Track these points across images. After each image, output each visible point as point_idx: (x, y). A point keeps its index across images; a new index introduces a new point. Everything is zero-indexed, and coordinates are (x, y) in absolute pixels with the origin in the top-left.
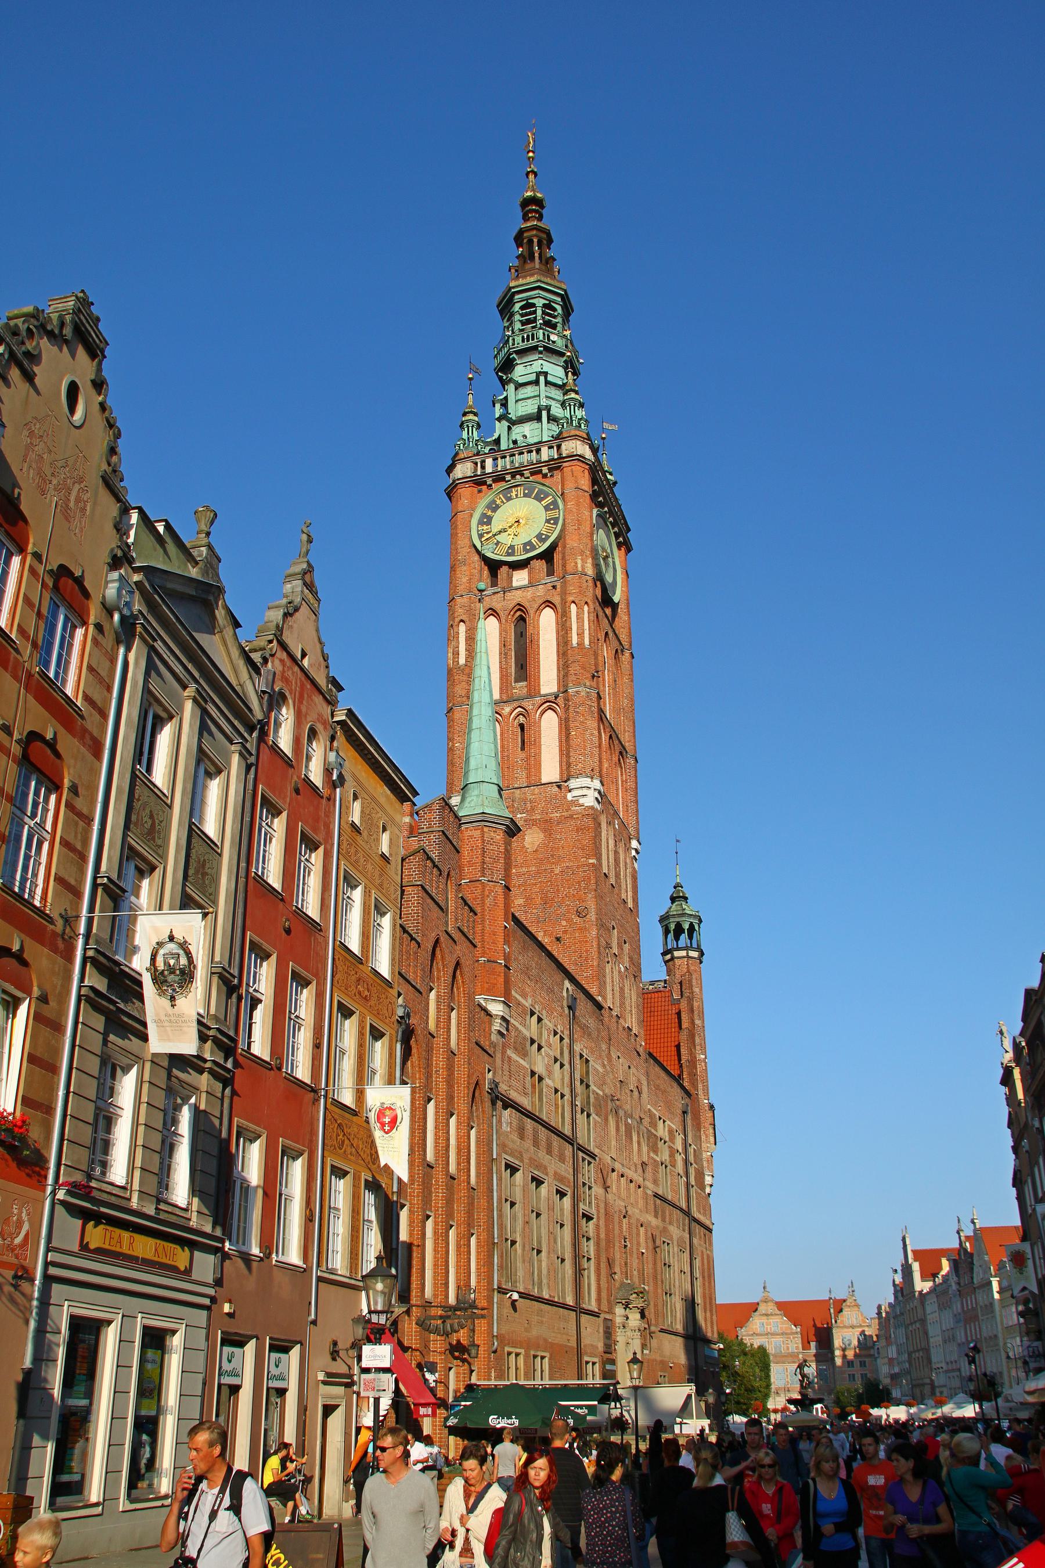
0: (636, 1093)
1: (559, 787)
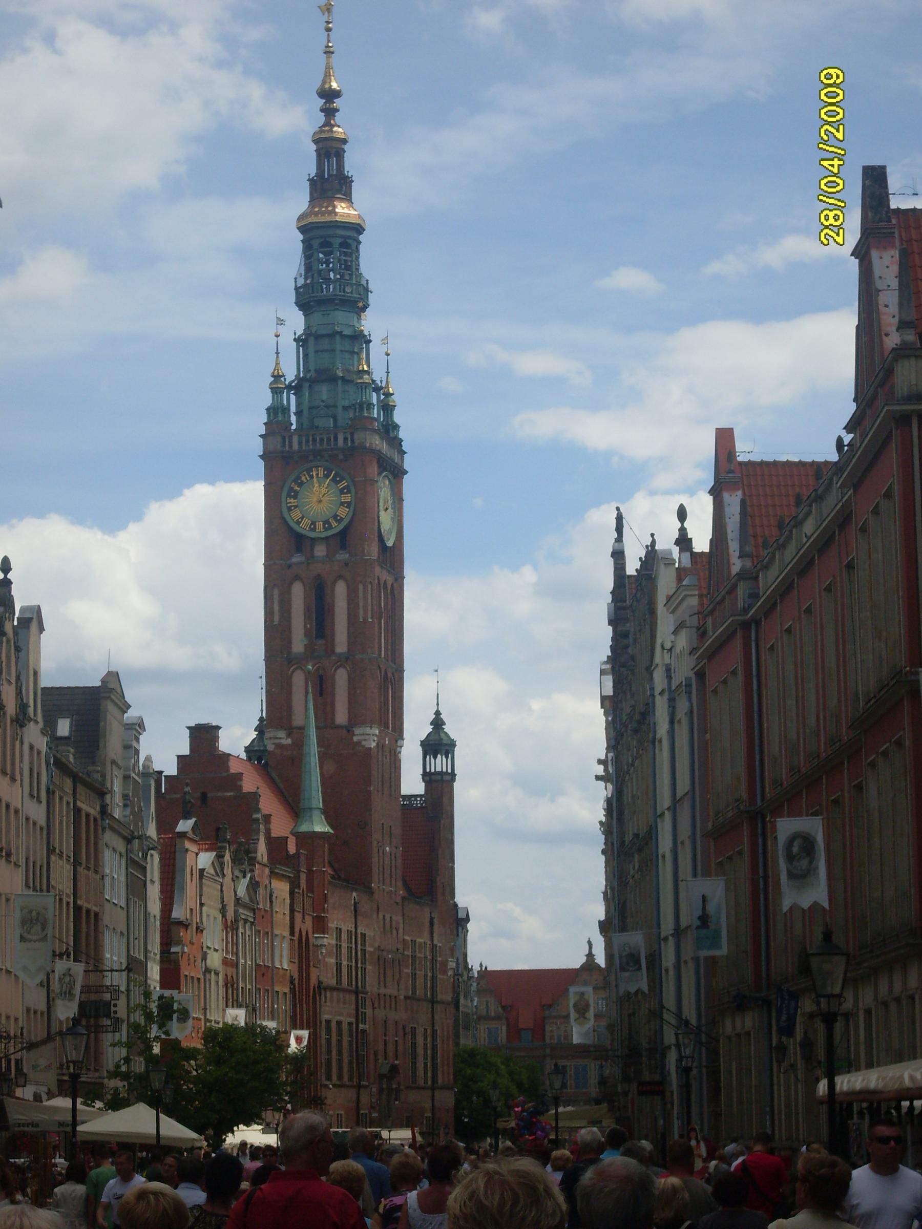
0: (394, 932)
1: (349, 731)
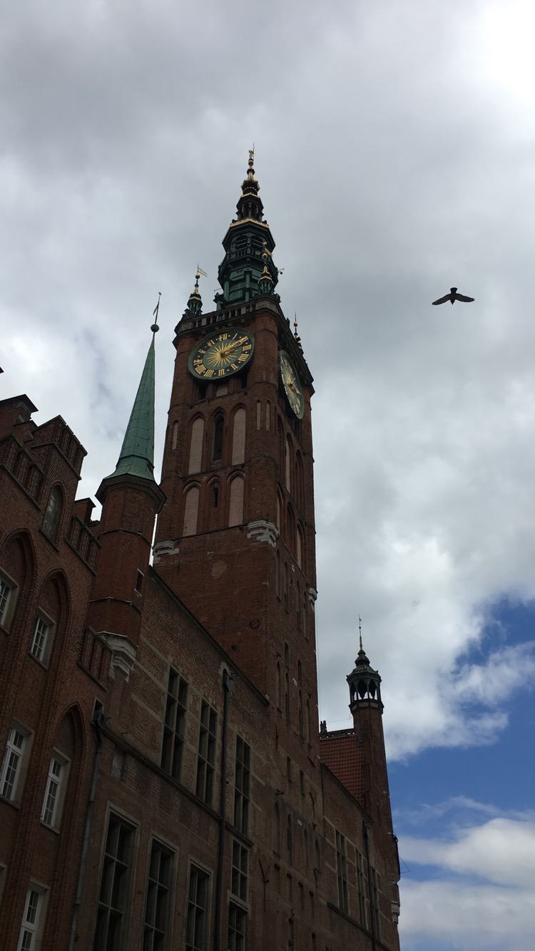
0: (308, 799)
